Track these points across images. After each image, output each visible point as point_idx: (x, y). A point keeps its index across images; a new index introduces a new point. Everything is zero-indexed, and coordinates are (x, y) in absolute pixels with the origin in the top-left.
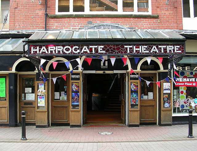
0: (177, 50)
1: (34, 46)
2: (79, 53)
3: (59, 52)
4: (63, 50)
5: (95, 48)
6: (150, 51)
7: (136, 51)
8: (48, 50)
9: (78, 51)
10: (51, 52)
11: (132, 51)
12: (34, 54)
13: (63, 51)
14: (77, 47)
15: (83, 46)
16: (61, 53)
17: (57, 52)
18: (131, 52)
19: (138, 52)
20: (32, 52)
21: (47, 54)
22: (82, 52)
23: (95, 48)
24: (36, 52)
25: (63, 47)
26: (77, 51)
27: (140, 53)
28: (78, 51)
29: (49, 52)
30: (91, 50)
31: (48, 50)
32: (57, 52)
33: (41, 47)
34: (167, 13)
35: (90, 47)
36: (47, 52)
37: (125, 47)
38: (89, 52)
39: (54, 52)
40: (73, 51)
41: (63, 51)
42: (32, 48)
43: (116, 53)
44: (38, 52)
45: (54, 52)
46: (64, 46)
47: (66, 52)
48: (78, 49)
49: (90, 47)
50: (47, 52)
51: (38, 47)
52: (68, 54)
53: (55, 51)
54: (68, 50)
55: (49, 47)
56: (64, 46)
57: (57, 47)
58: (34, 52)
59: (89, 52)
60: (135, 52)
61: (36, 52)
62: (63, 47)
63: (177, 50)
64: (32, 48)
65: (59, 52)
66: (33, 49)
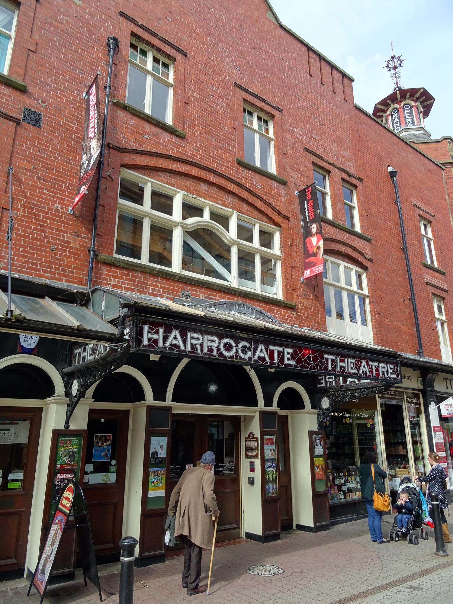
0: (288, 359)
1: (150, 323)
2: (250, 358)
3: (210, 350)
4: (219, 346)
5: (279, 352)
6: (358, 371)
7: (341, 367)
8: (165, 339)
9: (249, 354)
10: (193, 346)
11: (335, 366)
12: (150, 345)
13: (218, 350)
14: (247, 344)
15: (257, 342)
16: (215, 353)
17: (205, 350)
18: (333, 369)
19: (344, 371)
20: (145, 342)
21: (183, 351)
22: (256, 358)
23: (279, 352)
24: (156, 341)
25: (220, 340)
26: (246, 353)
27: (346, 373)
28: (249, 354)
29: (189, 348)
30: (271, 354)
31: (165, 339)
32: (205, 350)
33: (167, 331)
34: (306, 303)
35: (271, 347)
36: (182, 347)
37: (326, 356)
38: (268, 359)
39: (215, 350)
40: (240, 351)
41: (218, 350)
42: (146, 328)
43: (311, 368)
44: (161, 343)
45: (215, 350)
46: (221, 338)
47: (225, 353)
48: (249, 349)
49: (271, 347)
50: (182, 347)
51: (161, 330)
52: (229, 357)
53: (202, 346)
54: (228, 347)
55: (189, 335)
56: (221, 338)
57: (205, 336)
58: (149, 340)
59: (268, 359)
60: (339, 369)
61: (156, 341)
62: (220, 340)
63: (288, 359)
64: (146, 328)
65: (210, 350)
66: (149, 332)
